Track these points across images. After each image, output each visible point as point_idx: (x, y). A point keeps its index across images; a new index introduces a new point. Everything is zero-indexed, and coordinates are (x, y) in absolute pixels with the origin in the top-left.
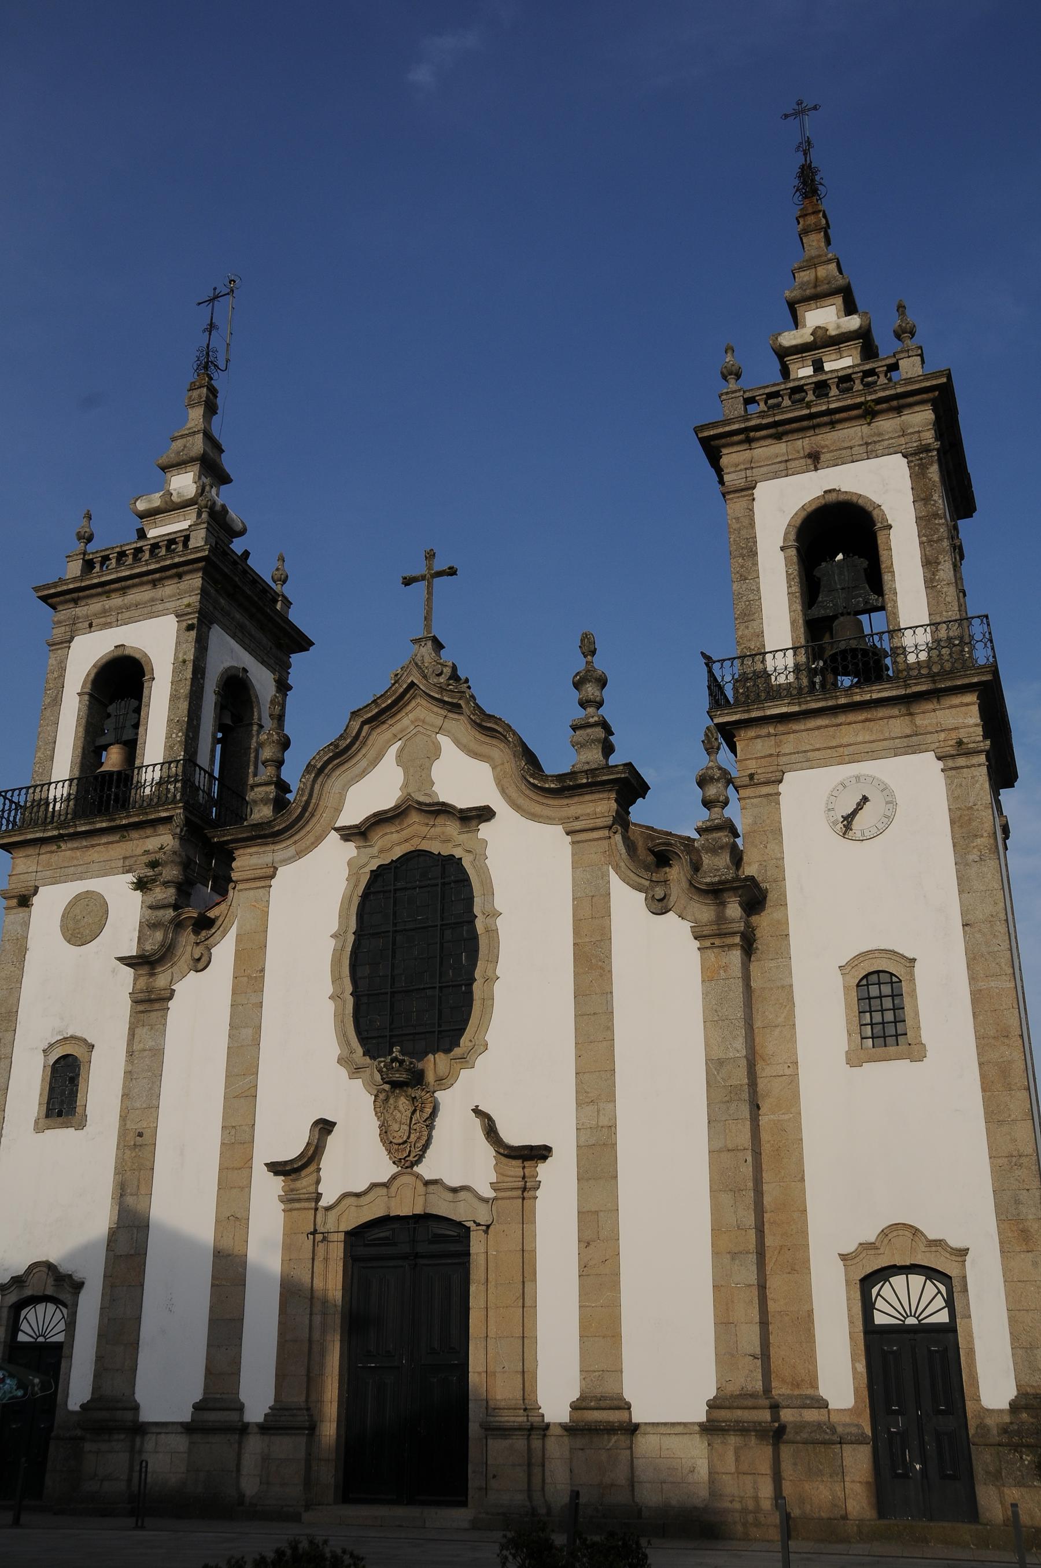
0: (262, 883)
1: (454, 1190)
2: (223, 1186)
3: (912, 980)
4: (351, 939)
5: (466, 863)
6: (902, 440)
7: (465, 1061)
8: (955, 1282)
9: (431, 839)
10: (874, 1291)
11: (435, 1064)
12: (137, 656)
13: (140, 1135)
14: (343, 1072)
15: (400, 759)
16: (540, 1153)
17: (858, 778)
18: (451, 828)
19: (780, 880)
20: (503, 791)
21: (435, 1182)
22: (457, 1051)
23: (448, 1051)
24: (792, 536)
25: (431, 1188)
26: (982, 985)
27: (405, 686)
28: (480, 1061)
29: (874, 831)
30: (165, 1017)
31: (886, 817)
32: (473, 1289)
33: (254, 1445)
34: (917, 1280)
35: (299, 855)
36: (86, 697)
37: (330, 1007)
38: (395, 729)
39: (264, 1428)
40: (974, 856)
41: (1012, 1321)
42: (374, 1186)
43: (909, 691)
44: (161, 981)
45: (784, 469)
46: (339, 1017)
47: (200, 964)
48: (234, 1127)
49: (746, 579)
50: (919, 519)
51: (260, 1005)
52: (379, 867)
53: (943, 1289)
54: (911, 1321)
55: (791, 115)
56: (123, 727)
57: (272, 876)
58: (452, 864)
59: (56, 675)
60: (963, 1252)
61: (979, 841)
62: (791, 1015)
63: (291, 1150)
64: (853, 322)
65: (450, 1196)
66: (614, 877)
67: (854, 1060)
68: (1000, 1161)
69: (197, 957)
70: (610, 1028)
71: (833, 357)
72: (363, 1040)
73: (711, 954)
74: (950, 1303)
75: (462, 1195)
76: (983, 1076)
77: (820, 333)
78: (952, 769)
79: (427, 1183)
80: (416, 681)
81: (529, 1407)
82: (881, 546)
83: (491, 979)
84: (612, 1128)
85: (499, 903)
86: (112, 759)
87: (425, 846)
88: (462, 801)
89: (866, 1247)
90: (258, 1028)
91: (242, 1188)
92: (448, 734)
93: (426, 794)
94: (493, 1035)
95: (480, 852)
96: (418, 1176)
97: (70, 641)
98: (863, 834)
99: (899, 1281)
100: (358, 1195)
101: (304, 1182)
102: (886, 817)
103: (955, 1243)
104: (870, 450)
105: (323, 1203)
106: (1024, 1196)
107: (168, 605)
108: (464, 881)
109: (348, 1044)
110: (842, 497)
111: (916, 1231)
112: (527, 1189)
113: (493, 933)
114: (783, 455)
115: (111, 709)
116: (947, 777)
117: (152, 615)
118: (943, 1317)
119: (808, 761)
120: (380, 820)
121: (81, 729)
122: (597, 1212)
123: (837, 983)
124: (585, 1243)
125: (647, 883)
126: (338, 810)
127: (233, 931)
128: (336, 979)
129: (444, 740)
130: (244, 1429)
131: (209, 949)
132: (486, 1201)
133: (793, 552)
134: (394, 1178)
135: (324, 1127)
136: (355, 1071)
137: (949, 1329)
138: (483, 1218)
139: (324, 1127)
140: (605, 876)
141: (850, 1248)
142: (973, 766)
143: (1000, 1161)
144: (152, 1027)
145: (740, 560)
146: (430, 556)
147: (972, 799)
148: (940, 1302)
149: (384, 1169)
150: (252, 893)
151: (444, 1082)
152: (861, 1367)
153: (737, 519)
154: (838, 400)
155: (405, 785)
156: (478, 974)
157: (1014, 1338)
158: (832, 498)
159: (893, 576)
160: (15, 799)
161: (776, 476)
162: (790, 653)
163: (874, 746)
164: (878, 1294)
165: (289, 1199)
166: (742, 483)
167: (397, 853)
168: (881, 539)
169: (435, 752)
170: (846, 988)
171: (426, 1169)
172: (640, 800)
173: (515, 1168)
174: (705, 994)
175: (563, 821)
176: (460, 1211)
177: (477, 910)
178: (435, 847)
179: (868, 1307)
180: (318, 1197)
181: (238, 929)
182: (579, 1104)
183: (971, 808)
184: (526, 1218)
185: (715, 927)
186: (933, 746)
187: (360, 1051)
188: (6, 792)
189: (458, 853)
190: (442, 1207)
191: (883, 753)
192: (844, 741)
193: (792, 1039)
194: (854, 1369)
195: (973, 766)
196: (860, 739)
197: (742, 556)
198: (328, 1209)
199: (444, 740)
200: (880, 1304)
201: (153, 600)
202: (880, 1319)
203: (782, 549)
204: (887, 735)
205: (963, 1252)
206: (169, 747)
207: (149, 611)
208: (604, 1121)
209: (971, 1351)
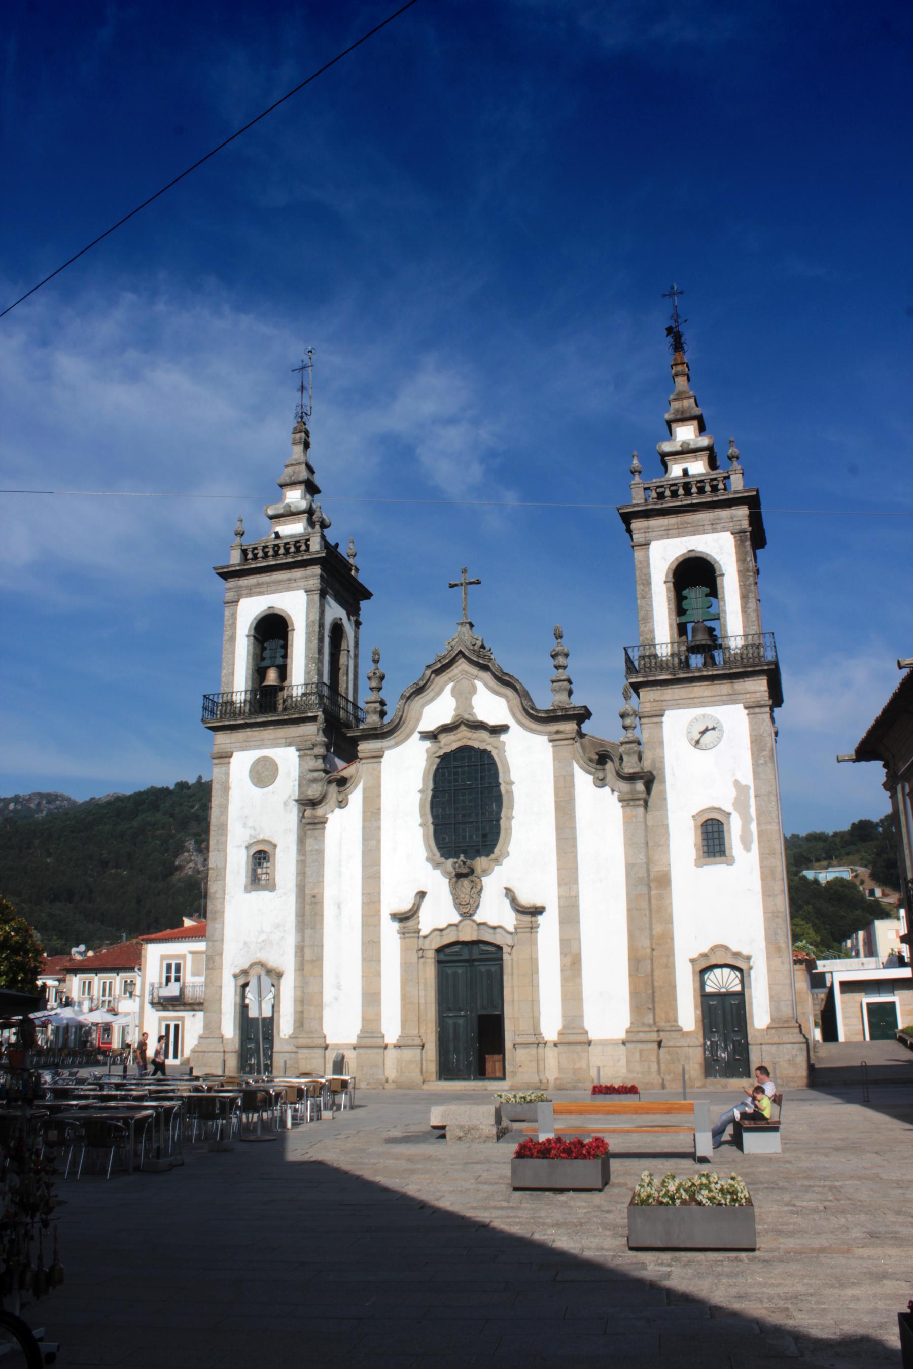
0: (376, 760)
1: (494, 928)
2: (365, 925)
3: (729, 824)
4: (430, 793)
5: (494, 754)
6: (731, 524)
7: (497, 861)
8: (745, 972)
9: (473, 740)
10: (706, 976)
11: (480, 863)
12: (283, 614)
13: (314, 897)
14: (429, 866)
15: (454, 693)
16: (537, 911)
17: (704, 716)
18: (484, 735)
19: (662, 769)
20: (514, 715)
21: (484, 924)
22: (492, 856)
23: (488, 855)
24: (671, 576)
25: (482, 927)
26: (763, 827)
27: (456, 652)
28: (506, 862)
29: (712, 745)
30: (323, 833)
31: (718, 738)
32: (505, 977)
33: (391, 1054)
34: (726, 971)
35: (397, 744)
36: (252, 638)
37: (420, 831)
38: (450, 675)
39: (397, 1046)
40: (761, 761)
41: (770, 989)
42: (450, 925)
43: (732, 671)
44: (320, 811)
45: (667, 534)
46: (425, 836)
47: (342, 804)
48: (369, 894)
49: (645, 598)
50: (739, 572)
51: (379, 828)
52: (445, 754)
53: (739, 975)
54: (723, 990)
55: (667, 295)
56: (275, 657)
57: (381, 757)
58: (485, 754)
59: (230, 622)
60: (748, 958)
61: (765, 753)
62: (668, 839)
63: (405, 906)
64: (704, 441)
65: (491, 931)
66: (576, 766)
67: (699, 864)
68: (769, 915)
69: (340, 800)
70: (575, 846)
71: (692, 460)
72: (440, 848)
73: (628, 809)
74: (742, 982)
75: (498, 930)
76: (762, 873)
77: (685, 446)
78: (752, 714)
79: (479, 925)
80: (463, 650)
81: (537, 1033)
82: (719, 586)
83: (510, 818)
84: (577, 897)
85: (514, 776)
86: (272, 677)
87: (470, 743)
88: (492, 721)
89: (704, 956)
90: (379, 841)
91: (375, 926)
92: (481, 680)
93: (469, 714)
94: (512, 848)
95: (501, 747)
96: (474, 921)
97: (238, 602)
98: (706, 746)
99: (717, 971)
100: (441, 930)
101: (410, 924)
102: (718, 738)
103: (745, 952)
104: (714, 528)
105: (422, 933)
106: (779, 931)
107: (300, 584)
108: (493, 763)
109: (431, 850)
110: (698, 555)
111: (726, 948)
112: (533, 928)
113: (510, 793)
114: (665, 526)
115: (266, 645)
116: (749, 719)
117: (289, 589)
118: (738, 988)
119: (678, 704)
120: (446, 729)
121: (250, 657)
122: (570, 940)
123: (691, 824)
124: (563, 954)
125: (594, 770)
126: (418, 720)
127: (360, 786)
128: (422, 815)
129: (479, 684)
130: (386, 1047)
131: (347, 796)
132: (511, 934)
133: (671, 585)
134: (461, 922)
135: (422, 895)
136: (437, 865)
137: (741, 995)
138: (510, 943)
139: (422, 895)
140: (571, 766)
141: (695, 955)
142: (763, 713)
143: (769, 915)
144: (316, 838)
145: (642, 587)
146: (465, 571)
147: (762, 731)
148: (737, 981)
149: (456, 918)
150: (370, 765)
151: (486, 872)
152: (699, 1012)
153: (640, 562)
154: (697, 499)
155: (456, 709)
156: (503, 815)
157: (771, 997)
158: (692, 555)
159: (725, 603)
160: (215, 700)
161: (662, 538)
162: (669, 646)
163: (713, 699)
164: (708, 978)
165: (403, 933)
166: (642, 540)
167: (454, 746)
168: (718, 582)
169: (474, 690)
170: (696, 827)
171: (478, 917)
172: (587, 721)
173: (527, 918)
174: (625, 830)
175: (549, 734)
176: (498, 939)
177: (501, 780)
178: (476, 745)
179: (703, 984)
180: (419, 931)
181: (364, 785)
182: (559, 885)
183: (761, 735)
184: (534, 943)
185: (630, 796)
186: (745, 701)
187: (438, 854)
188: (210, 695)
189: (489, 748)
190: (487, 936)
191: (718, 703)
192: (697, 695)
193: (667, 852)
194: (695, 1012)
195: (763, 713)
196: (705, 694)
197: (643, 584)
198: (425, 937)
199: (479, 684)
200: (708, 982)
201: (289, 580)
202: (708, 989)
203: (665, 582)
204: (719, 693)
205: (748, 958)
206: (307, 673)
207: (288, 586)
208: (573, 894)
209: (751, 1004)
